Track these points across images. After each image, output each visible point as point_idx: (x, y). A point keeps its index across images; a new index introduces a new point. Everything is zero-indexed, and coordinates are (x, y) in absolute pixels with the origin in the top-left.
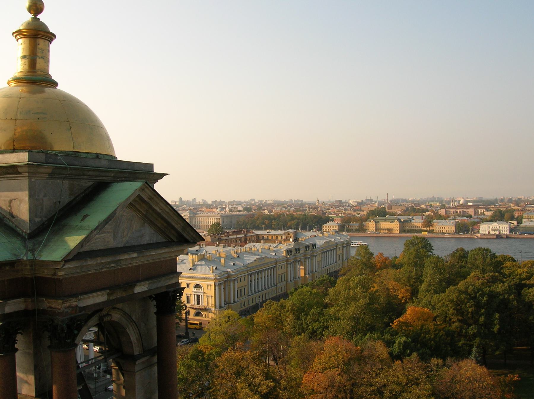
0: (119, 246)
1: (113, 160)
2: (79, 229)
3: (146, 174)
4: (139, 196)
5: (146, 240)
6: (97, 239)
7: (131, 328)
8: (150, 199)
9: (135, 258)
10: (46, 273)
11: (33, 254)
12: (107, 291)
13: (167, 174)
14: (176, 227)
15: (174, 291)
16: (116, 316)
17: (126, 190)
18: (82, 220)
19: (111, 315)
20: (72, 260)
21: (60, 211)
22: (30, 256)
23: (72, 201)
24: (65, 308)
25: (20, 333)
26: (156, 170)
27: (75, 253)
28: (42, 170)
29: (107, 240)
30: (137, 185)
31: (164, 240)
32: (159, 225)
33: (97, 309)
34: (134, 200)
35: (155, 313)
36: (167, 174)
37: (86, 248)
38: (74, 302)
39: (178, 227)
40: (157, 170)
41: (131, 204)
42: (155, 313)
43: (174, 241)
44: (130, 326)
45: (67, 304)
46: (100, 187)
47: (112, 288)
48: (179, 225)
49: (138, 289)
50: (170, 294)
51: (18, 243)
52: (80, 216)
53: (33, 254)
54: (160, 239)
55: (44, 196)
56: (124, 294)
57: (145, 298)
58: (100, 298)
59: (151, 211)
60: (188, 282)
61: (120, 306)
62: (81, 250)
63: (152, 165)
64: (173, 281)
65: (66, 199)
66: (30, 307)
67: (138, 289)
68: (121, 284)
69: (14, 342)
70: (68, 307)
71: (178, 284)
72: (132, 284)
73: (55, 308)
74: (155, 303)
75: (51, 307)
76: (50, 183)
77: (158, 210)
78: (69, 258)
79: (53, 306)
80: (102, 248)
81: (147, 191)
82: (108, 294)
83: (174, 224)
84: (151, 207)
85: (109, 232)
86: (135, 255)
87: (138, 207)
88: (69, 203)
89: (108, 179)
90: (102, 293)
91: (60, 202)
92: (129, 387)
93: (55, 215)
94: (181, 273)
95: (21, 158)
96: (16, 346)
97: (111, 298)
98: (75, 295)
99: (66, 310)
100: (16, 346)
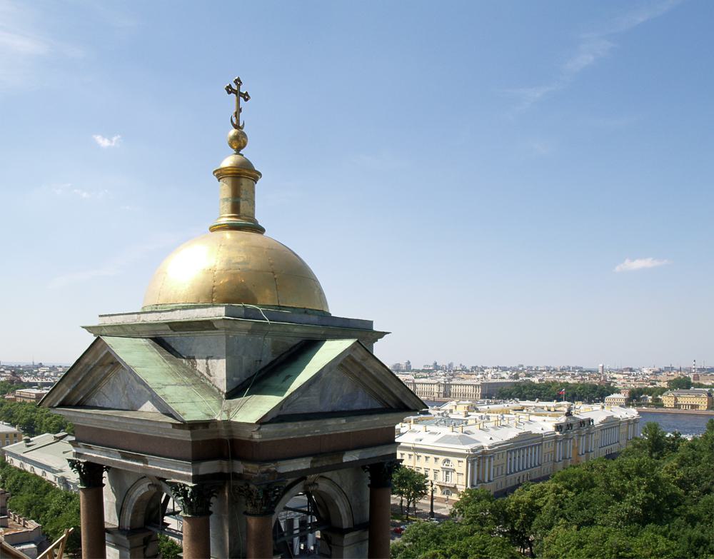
0: (327, 410)
1: (325, 315)
2: (279, 391)
3: (363, 333)
4: (349, 356)
5: (358, 405)
6: (301, 402)
7: (340, 500)
8: (363, 360)
9: (344, 424)
10: (244, 435)
11: (228, 415)
12: (310, 459)
13: (388, 333)
14: (394, 391)
15: (391, 463)
16: (323, 486)
17: (331, 350)
18: (284, 381)
19: (317, 484)
20: (271, 422)
21: (260, 371)
22: (225, 417)
23: (276, 360)
24: (262, 473)
25: (215, 496)
26: (376, 328)
27: (274, 415)
28: (240, 326)
29: (314, 403)
30: (347, 343)
31: (380, 407)
32: (374, 390)
33: (301, 476)
34: (345, 360)
35: (369, 486)
36: (388, 333)
37: (288, 411)
38: (272, 467)
39: (397, 393)
40: (376, 328)
41: (341, 365)
42: (369, 486)
43: (392, 408)
44: (339, 497)
45: (264, 469)
46: (309, 346)
47: (316, 455)
48: (398, 391)
49: (348, 457)
50: (385, 465)
51: (213, 402)
52: (282, 376)
53: (228, 415)
54: (377, 405)
55: (243, 355)
56: (331, 463)
57: (359, 466)
58: (303, 464)
59: (364, 373)
60: (403, 452)
61: (328, 474)
62: (282, 413)
63: (372, 322)
64: (390, 452)
65: (268, 358)
66: (226, 471)
67: (348, 457)
68: (326, 453)
69: (209, 504)
70: (266, 472)
71: (395, 454)
72: (341, 452)
73: (252, 473)
74: (368, 474)
75: (248, 472)
76: (250, 340)
77: (373, 373)
78: (265, 420)
79: (250, 470)
80: (306, 412)
81: (360, 351)
82: (312, 462)
83: (391, 389)
84: (364, 369)
85: (315, 395)
86: (343, 421)
87: (349, 368)
88: (272, 363)
89: (319, 337)
90: (304, 460)
91: (260, 361)
92: (201, 538)
93: (254, 375)
94: (399, 443)
95: (218, 312)
96: (211, 509)
97: (315, 465)
98: (275, 460)
99: (262, 476)
100: (211, 509)
